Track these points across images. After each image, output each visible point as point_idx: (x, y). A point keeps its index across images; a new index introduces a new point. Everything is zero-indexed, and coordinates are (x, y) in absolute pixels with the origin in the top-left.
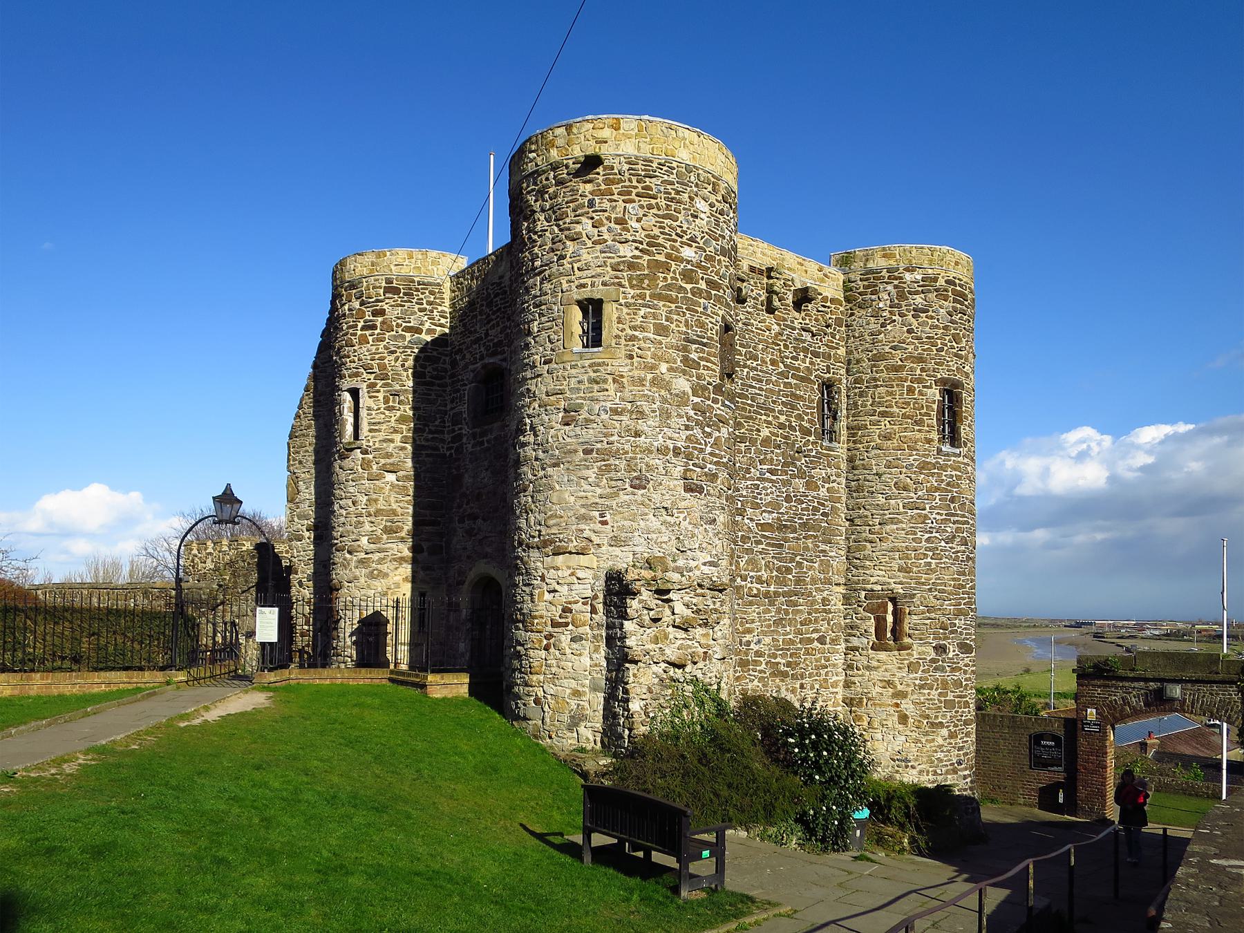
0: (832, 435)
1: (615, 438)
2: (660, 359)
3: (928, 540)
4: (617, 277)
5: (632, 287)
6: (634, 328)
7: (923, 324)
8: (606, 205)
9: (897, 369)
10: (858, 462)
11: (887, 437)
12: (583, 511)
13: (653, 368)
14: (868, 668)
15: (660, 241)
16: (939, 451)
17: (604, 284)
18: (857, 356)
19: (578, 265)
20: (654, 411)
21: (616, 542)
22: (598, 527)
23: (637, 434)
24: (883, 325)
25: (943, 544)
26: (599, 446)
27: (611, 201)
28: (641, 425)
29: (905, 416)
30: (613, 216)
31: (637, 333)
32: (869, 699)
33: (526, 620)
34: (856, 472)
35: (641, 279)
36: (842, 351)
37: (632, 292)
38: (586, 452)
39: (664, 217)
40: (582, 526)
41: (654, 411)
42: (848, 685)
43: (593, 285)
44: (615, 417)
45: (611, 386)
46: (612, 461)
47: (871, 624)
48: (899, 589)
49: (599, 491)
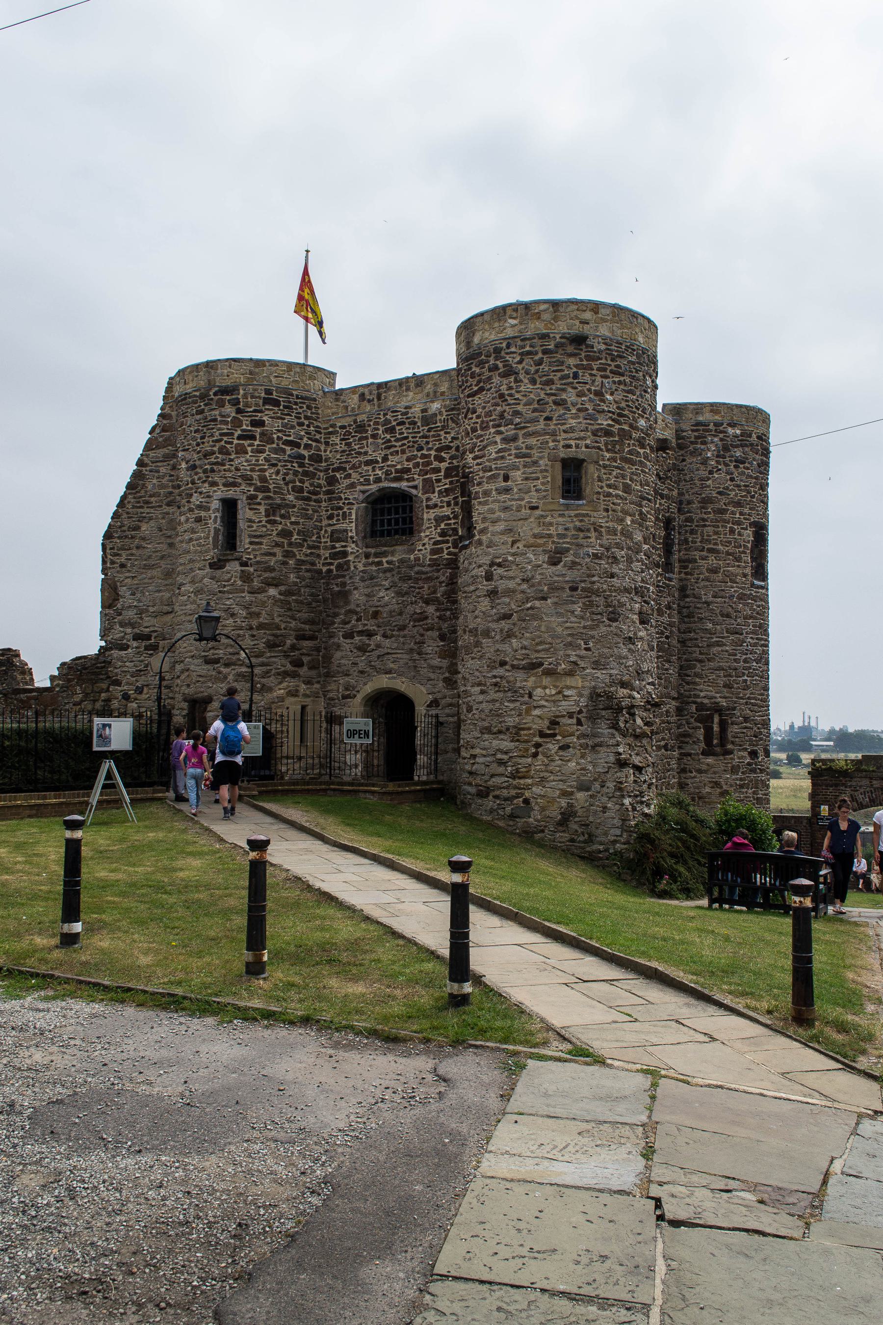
1: (595, 579)
2: (626, 513)
3: (745, 661)
4: (597, 442)
5: (608, 451)
6: (609, 486)
7: (743, 473)
8: (587, 378)
9: (722, 511)
10: (688, 592)
11: (714, 571)
12: (570, 639)
13: (622, 520)
14: (700, 771)
15: (626, 412)
16: (753, 585)
17: (587, 447)
18: (687, 497)
19: (564, 427)
20: (623, 557)
21: (596, 665)
22: (583, 653)
23: (612, 576)
24: (711, 472)
25: (755, 664)
26: (583, 585)
27: (591, 375)
28: (615, 569)
29: (728, 553)
30: (593, 388)
31: (611, 490)
32: (700, 798)
33: (516, 733)
34: (688, 600)
35: (614, 443)
36: (675, 493)
37: (608, 455)
38: (573, 589)
39: (628, 392)
40: (569, 652)
41: (623, 557)
43: (577, 446)
44: (596, 561)
45: (593, 534)
46: (594, 598)
47: (700, 734)
49: (583, 623)
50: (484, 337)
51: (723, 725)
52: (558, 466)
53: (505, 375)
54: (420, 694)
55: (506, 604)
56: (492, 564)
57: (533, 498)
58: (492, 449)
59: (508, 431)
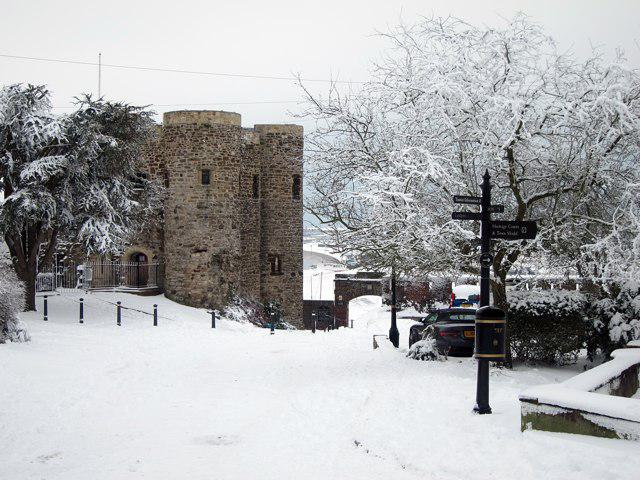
0: (256, 195)
28: (222, 209)
33: (185, 271)
42: (262, 288)
48: (279, 253)
50: (174, 121)
51: (279, 261)
52: (201, 172)
53: (181, 137)
54: (149, 253)
55: (180, 222)
56: (176, 207)
57: (191, 183)
58: (176, 164)
59: (182, 157)
